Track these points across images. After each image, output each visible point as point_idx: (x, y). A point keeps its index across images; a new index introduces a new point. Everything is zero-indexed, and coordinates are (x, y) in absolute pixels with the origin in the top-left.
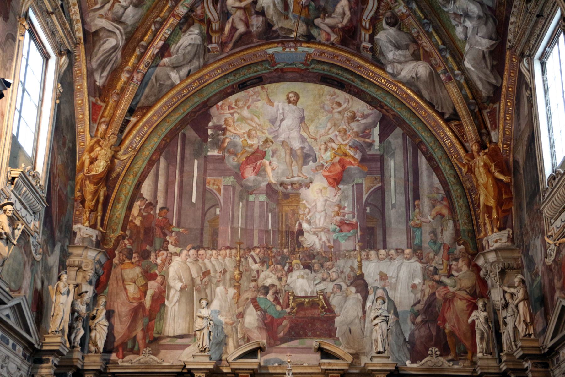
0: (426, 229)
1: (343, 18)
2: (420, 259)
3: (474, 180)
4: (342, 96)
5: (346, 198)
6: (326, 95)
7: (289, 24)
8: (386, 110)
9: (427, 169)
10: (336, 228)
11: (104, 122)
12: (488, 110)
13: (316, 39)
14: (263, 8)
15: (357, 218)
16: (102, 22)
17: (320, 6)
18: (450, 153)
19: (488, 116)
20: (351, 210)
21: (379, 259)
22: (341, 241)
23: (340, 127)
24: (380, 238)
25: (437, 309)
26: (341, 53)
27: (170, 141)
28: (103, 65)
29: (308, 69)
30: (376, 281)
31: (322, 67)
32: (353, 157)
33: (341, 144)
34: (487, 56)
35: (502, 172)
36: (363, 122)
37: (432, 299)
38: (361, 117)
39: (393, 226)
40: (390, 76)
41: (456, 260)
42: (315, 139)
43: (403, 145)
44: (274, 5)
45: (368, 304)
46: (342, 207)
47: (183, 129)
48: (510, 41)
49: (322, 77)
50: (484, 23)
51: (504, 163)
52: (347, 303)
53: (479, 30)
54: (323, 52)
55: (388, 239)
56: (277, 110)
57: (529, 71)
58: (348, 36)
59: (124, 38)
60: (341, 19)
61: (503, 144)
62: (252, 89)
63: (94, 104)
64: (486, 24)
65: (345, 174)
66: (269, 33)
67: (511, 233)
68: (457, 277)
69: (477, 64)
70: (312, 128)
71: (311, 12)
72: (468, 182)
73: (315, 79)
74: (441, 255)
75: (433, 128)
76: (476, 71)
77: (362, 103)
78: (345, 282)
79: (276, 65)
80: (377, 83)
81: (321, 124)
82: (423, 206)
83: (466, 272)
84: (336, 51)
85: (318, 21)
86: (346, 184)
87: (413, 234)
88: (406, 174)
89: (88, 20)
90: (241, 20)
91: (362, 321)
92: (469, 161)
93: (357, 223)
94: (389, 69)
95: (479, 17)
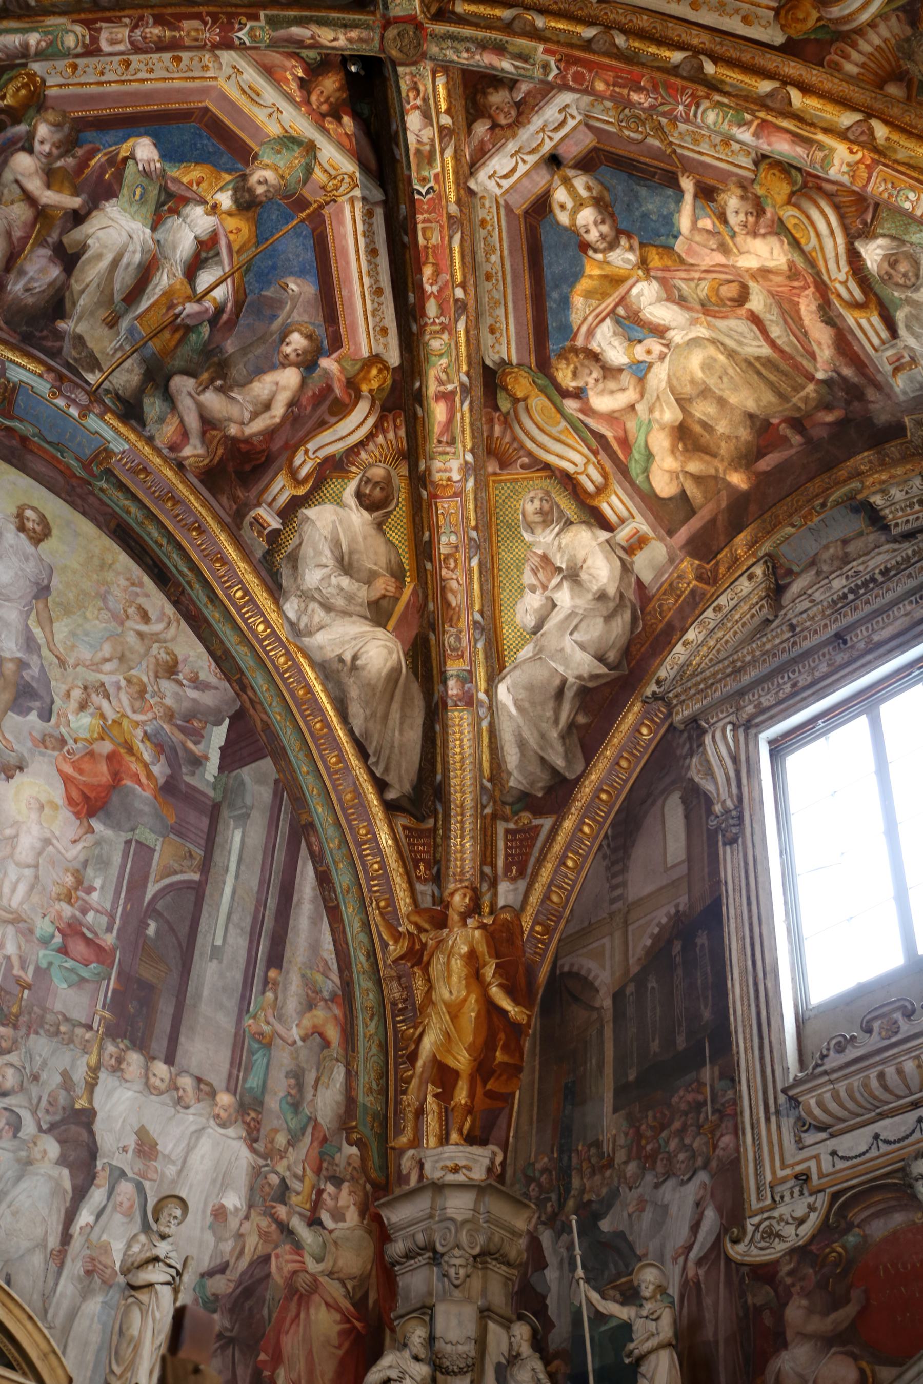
0: (283, 1058)
1: (255, 415)
2: (252, 1138)
3: (419, 984)
4: (157, 601)
5: (103, 863)
6: (119, 573)
7: (102, 341)
8: (251, 701)
9: (313, 901)
10: (53, 936)
12: (512, 826)
13: (144, 425)
14: (84, 248)
15: (118, 937)
17: (219, 349)
18: (370, 891)
19: (506, 840)
20: (108, 906)
21: (148, 1087)
22: (56, 980)
23: (133, 672)
24: (163, 1024)
25: (265, 1312)
26: (192, 498)
30: (125, 1150)
32: (146, 765)
33: (124, 715)
34: (569, 694)
35: (510, 991)
36: (193, 694)
37: (259, 1273)
38: (190, 680)
39: (205, 1008)
40: (286, 625)
41: (337, 1181)
42: (62, 663)
43: (272, 808)
44: (115, 263)
45: (85, 1217)
46: (86, 884)
48: (659, 683)
49: (118, 526)
50: (605, 613)
51: (521, 969)
52: (24, 1184)
53: (583, 626)
54: (145, 469)
55: (182, 1039)
57: (735, 760)
58: (238, 468)
60: (247, 415)
61: (536, 922)
64: (608, 619)
65: (115, 799)
66: (39, 325)
67: (499, 1159)
68: (331, 1232)
69: (533, 704)
70: (61, 629)
71: (185, 351)
72: (395, 984)
73: (100, 518)
74: (304, 1151)
75: (344, 810)
76: (520, 721)
77: (201, 649)
78: (34, 1113)
79: (11, 418)
80: (242, 625)
81: (87, 634)
82: (285, 989)
83: (352, 1229)
84: (181, 486)
85: (182, 384)
86: (112, 827)
87: (248, 1058)
88: (264, 883)
90: (9, 234)
91: (53, 1267)
92: (421, 930)
93: (114, 950)
94: (291, 608)
95: (602, 596)
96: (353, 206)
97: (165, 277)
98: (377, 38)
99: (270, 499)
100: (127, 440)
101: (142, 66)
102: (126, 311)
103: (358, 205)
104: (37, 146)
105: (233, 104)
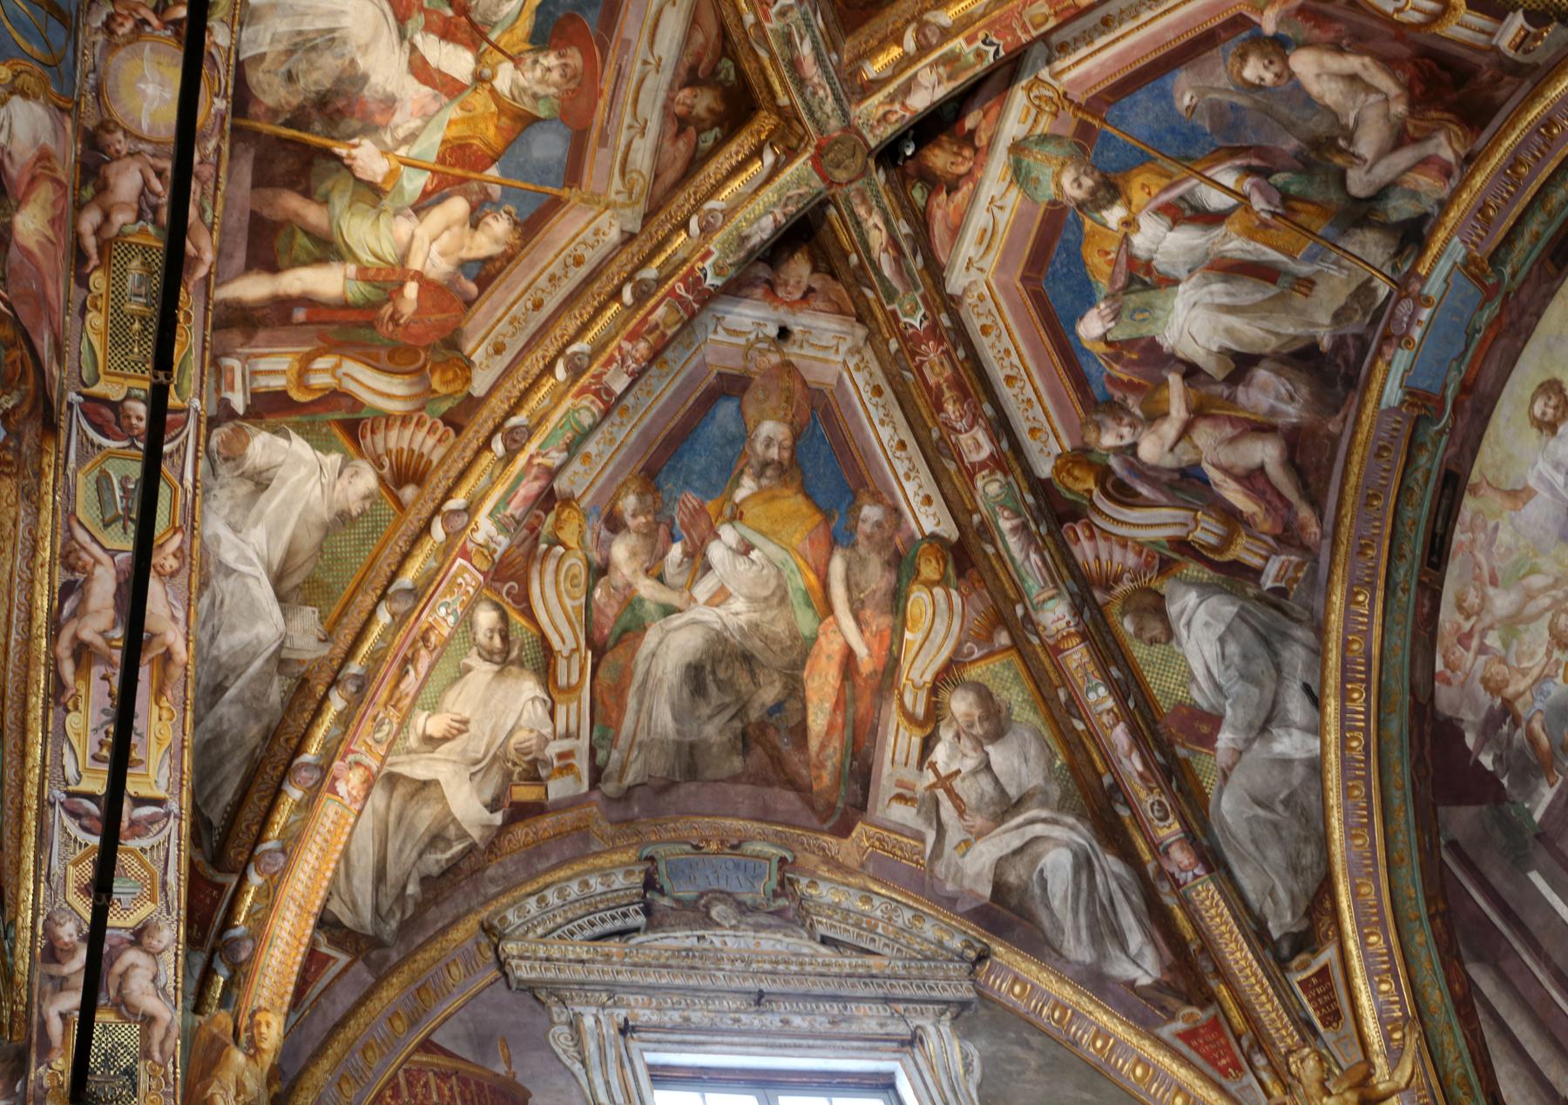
7: (1335, 287)
11: (1251, 1046)
13: (1425, 217)
16: (982, 853)
27: (1446, 901)
28: (1104, 929)
29: (1507, 294)
31: (1527, 236)
44: (1231, 310)
47: (1438, 834)
49: (1552, 258)
54: (1480, 211)
56: (1552, 488)
59: (1071, 820)
62: (1458, 527)
63: (1186, 1036)
71: (1315, 192)
73: (1545, 287)
79: (1443, 399)
85: (1359, 182)
89: (950, 887)
96: (1062, 71)
97: (1230, 246)
98: (853, 186)
99: (1483, 37)
100: (1447, 241)
101: (1006, 363)
102: (1287, 273)
103: (1058, 65)
104: (1128, 440)
105: (1006, 254)
